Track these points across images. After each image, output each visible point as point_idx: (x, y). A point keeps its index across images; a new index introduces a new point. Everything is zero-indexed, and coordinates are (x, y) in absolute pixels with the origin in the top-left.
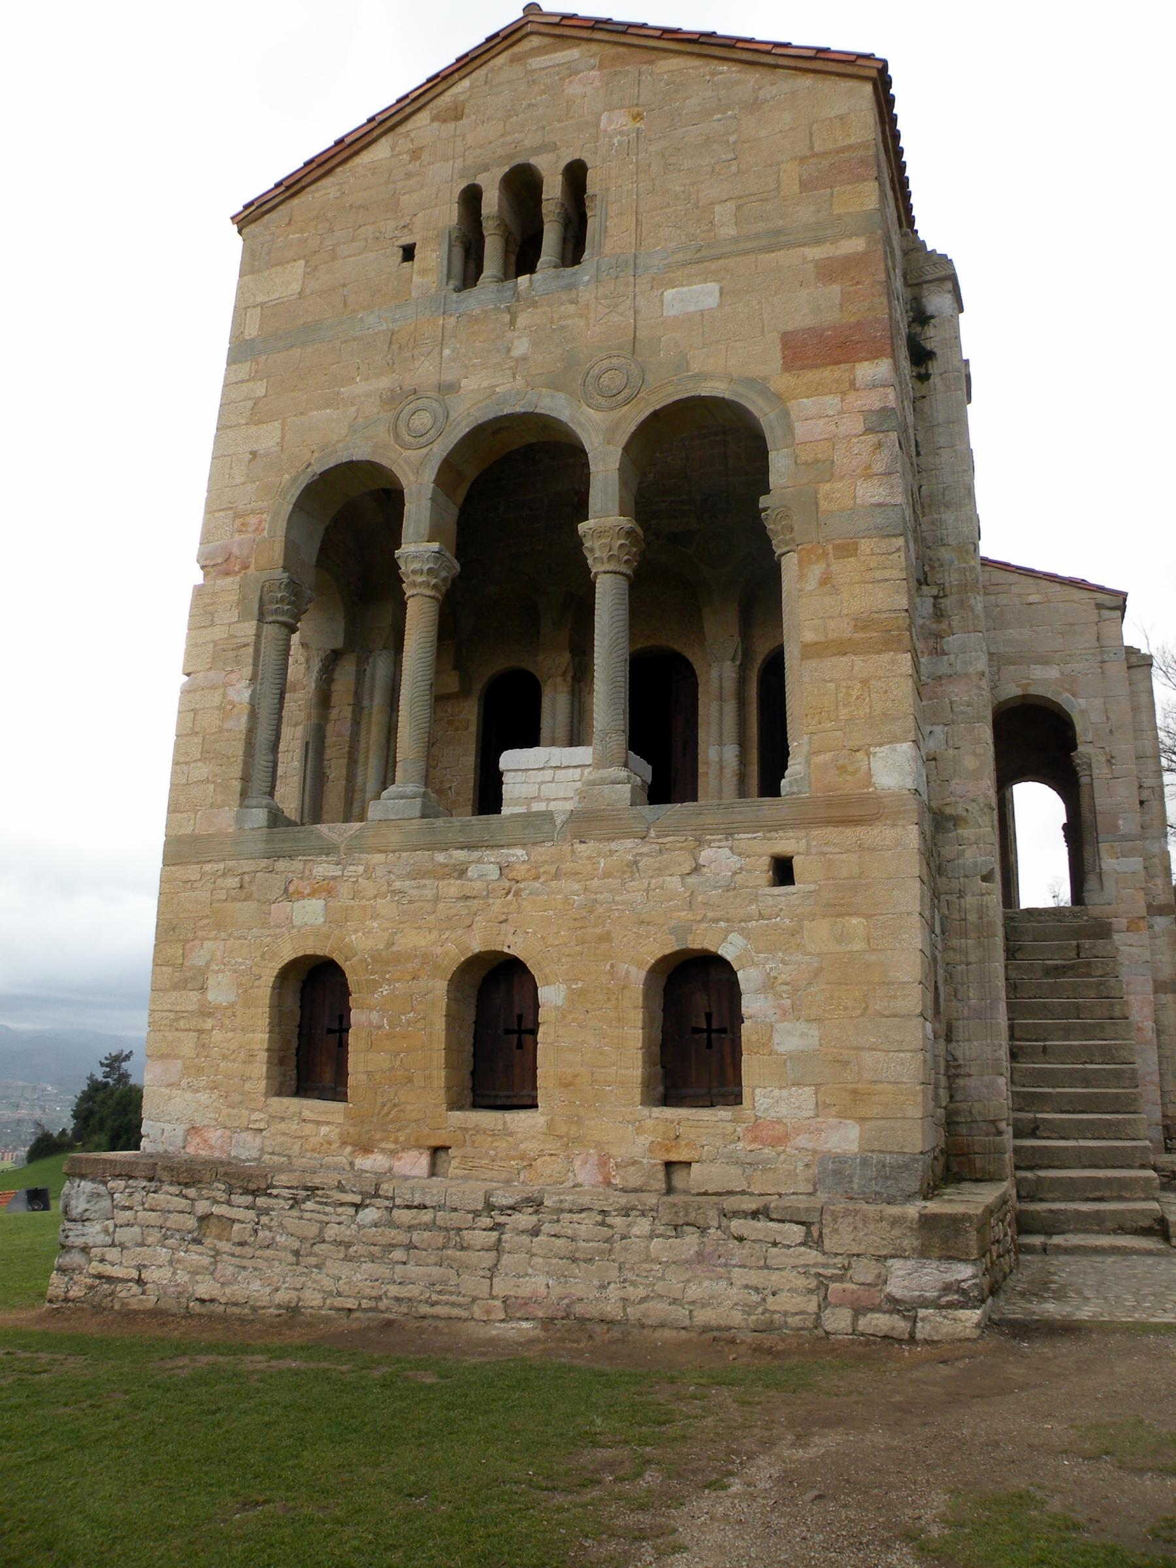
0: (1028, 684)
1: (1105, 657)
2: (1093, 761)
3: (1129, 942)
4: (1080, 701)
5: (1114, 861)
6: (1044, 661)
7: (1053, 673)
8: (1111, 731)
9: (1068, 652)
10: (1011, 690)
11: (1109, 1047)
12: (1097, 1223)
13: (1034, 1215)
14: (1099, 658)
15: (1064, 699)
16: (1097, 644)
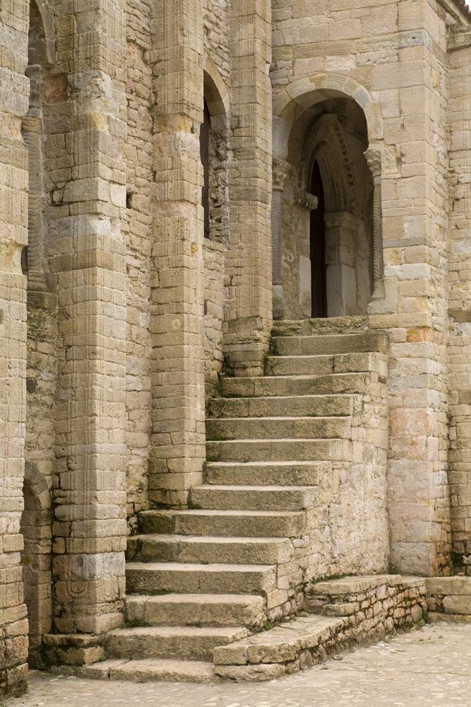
0: (322, 78)
1: (404, 43)
2: (383, 159)
3: (407, 353)
4: (374, 93)
5: (398, 267)
6: (341, 52)
7: (348, 64)
8: (403, 126)
9: (365, 40)
10: (303, 85)
11: (293, 469)
12: (173, 650)
13: (121, 640)
14: (396, 44)
15: (357, 92)
16: (396, 29)
